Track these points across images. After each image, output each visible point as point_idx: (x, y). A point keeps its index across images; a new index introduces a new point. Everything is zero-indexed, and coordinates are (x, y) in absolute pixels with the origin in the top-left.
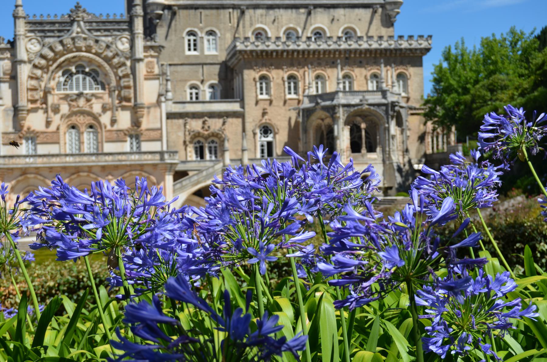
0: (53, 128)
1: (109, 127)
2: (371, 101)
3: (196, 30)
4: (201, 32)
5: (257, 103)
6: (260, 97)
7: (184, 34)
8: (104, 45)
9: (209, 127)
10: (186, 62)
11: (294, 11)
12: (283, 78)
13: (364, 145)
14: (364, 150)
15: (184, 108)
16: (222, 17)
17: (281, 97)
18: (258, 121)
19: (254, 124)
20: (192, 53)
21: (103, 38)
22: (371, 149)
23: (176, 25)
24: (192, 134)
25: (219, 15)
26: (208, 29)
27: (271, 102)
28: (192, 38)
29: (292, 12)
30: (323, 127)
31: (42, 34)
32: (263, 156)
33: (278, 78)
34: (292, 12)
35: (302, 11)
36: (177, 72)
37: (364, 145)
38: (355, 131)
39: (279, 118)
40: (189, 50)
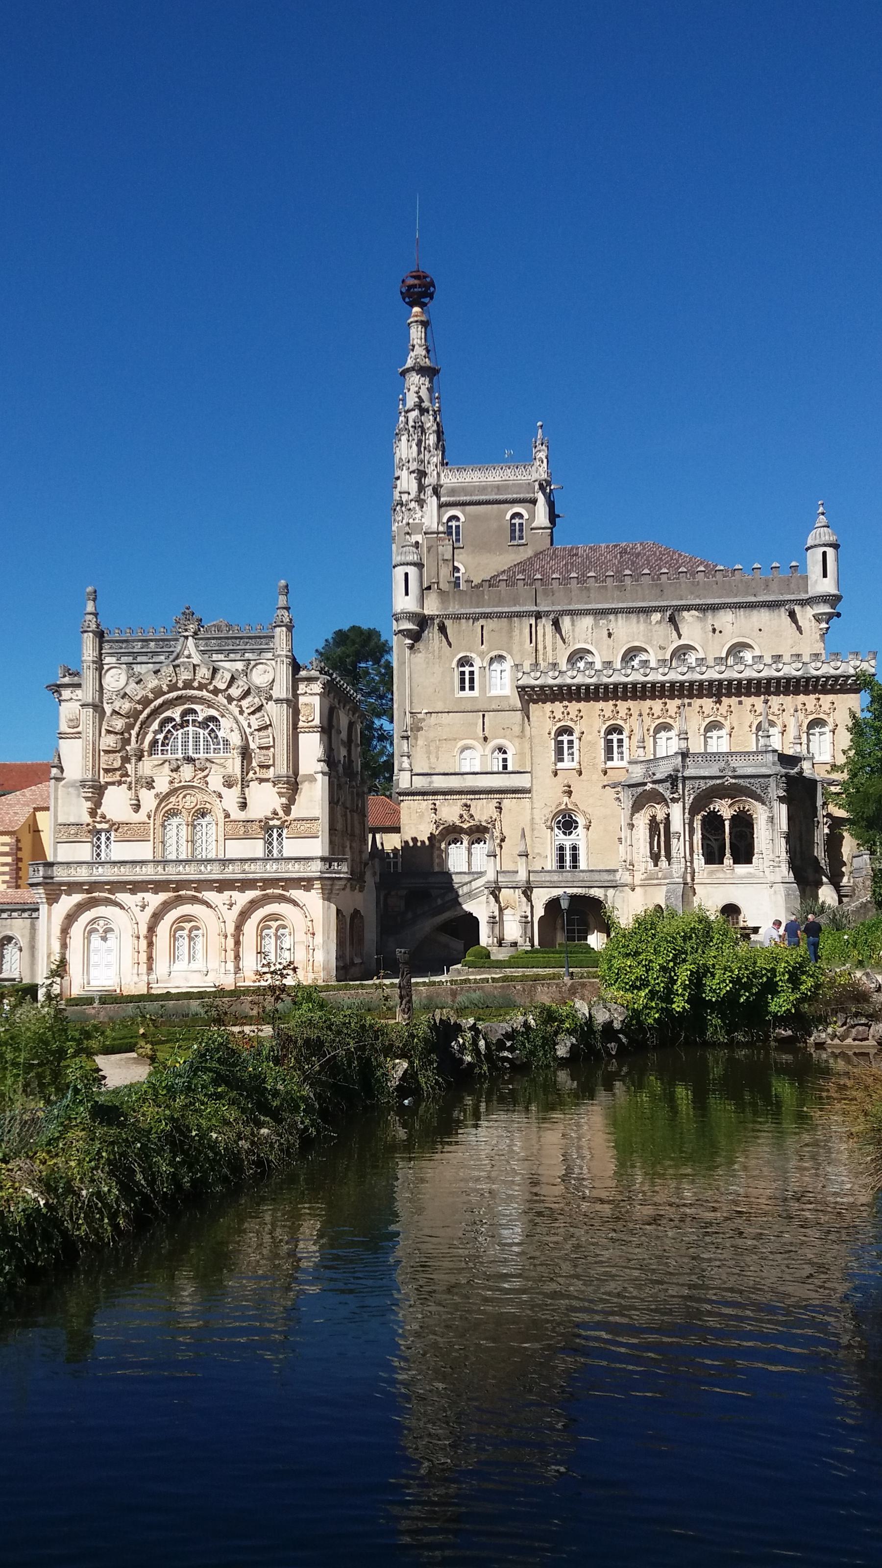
0: (141, 816)
1: (236, 814)
2: (740, 772)
3: (473, 655)
4: (482, 661)
7: (454, 664)
8: (228, 676)
9: (472, 816)
11: (642, 617)
14: (728, 860)
15: (431, 782)
16: (516, 632)
18: (554, 806)
20: (467, 693)
21: (227, 665)
25: (511, 630)
26: (493, 654)
28: (467, 669)
29: (638, 622)
30: (659, 818)
31: (130, 659)
32: (562, 867)
33: (590, 733)
34: (638, 622)
35: (656, 617)
38: (713, 823)
40: (463, 688)
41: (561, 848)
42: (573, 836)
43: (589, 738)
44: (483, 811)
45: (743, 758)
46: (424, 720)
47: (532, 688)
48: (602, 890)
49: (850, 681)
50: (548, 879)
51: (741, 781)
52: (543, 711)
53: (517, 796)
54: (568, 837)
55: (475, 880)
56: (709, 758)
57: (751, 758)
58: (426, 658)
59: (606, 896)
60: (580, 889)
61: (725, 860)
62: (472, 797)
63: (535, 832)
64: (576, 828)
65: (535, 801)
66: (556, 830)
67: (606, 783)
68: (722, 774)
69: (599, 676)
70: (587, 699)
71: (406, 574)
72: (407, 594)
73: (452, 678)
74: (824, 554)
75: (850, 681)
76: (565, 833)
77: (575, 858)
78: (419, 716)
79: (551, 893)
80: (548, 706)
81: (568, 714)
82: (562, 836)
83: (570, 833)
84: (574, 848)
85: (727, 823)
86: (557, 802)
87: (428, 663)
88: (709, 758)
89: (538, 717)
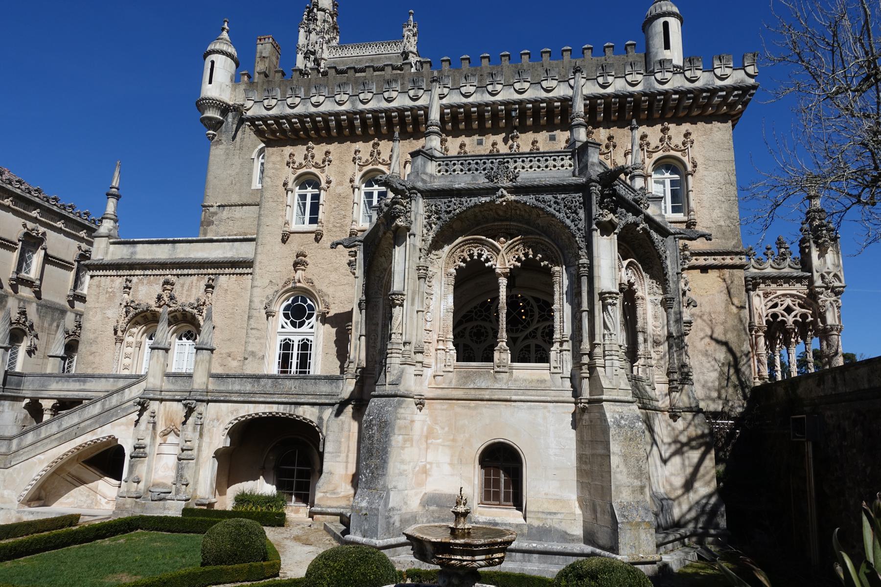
5: (284, 241)
6: (294, 227)
9: (172, 298)
10: (250, 202)
12: (352, 181)
13: (503, 335)
14: (502, 355)
17: (342, 226)
18: (281, 285)
19: (270, 291)
22: (532, 347)
23: (242, 140)
24: (132, 312)
27: (318, 237)
33: (340, 183)
36: (232, 219)
37: (503, 335)
39: (333, 276)
41: (287, 346)
42: (305, 328)
43: (340, 190)
44: (189, 291)
45: (535, 163)
46: (215, 213)
47: (264, 119)
48: (316, 409)
49: (716, 100)
50: (237, 387)
51: (529, 199)
52: (282, 155)
53: (238, 271)
54: (297, 330)
55: (129, 386)
56: (473, 166)
57: (551, 163)
58: (227, 149)
59: (320, 419)
60: (282, 407)
61: (496, 355)
62: (179, 272)
63: (252, 321)
64: (310, 316)
65: (257, 276)
66: (282, 319)
67: (336, 240)
68: (491, 185)
69: (353, 103)
70: (341, 139)
71: (213, 62)
72: (210, 82)
73: (251, 170)
74: (666, 25)
75: (716, 100)
76: (293, 324)
77: (304, 362)
78: (211, 209)
79: (237, 410)
80: (288, 150)
81: (313, 157)
82: (290, 328)
83: (301, 324)
84: (305, 346)
85: (503, 282)
86: (285, 279)
87: (228, 154)
88: (473, 166)
89: (274, 164)
